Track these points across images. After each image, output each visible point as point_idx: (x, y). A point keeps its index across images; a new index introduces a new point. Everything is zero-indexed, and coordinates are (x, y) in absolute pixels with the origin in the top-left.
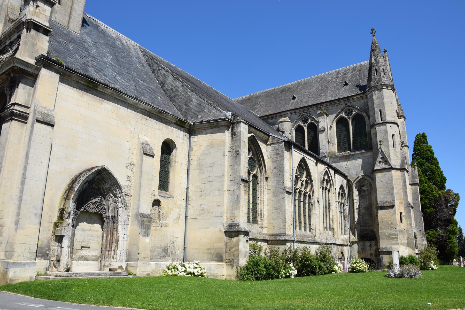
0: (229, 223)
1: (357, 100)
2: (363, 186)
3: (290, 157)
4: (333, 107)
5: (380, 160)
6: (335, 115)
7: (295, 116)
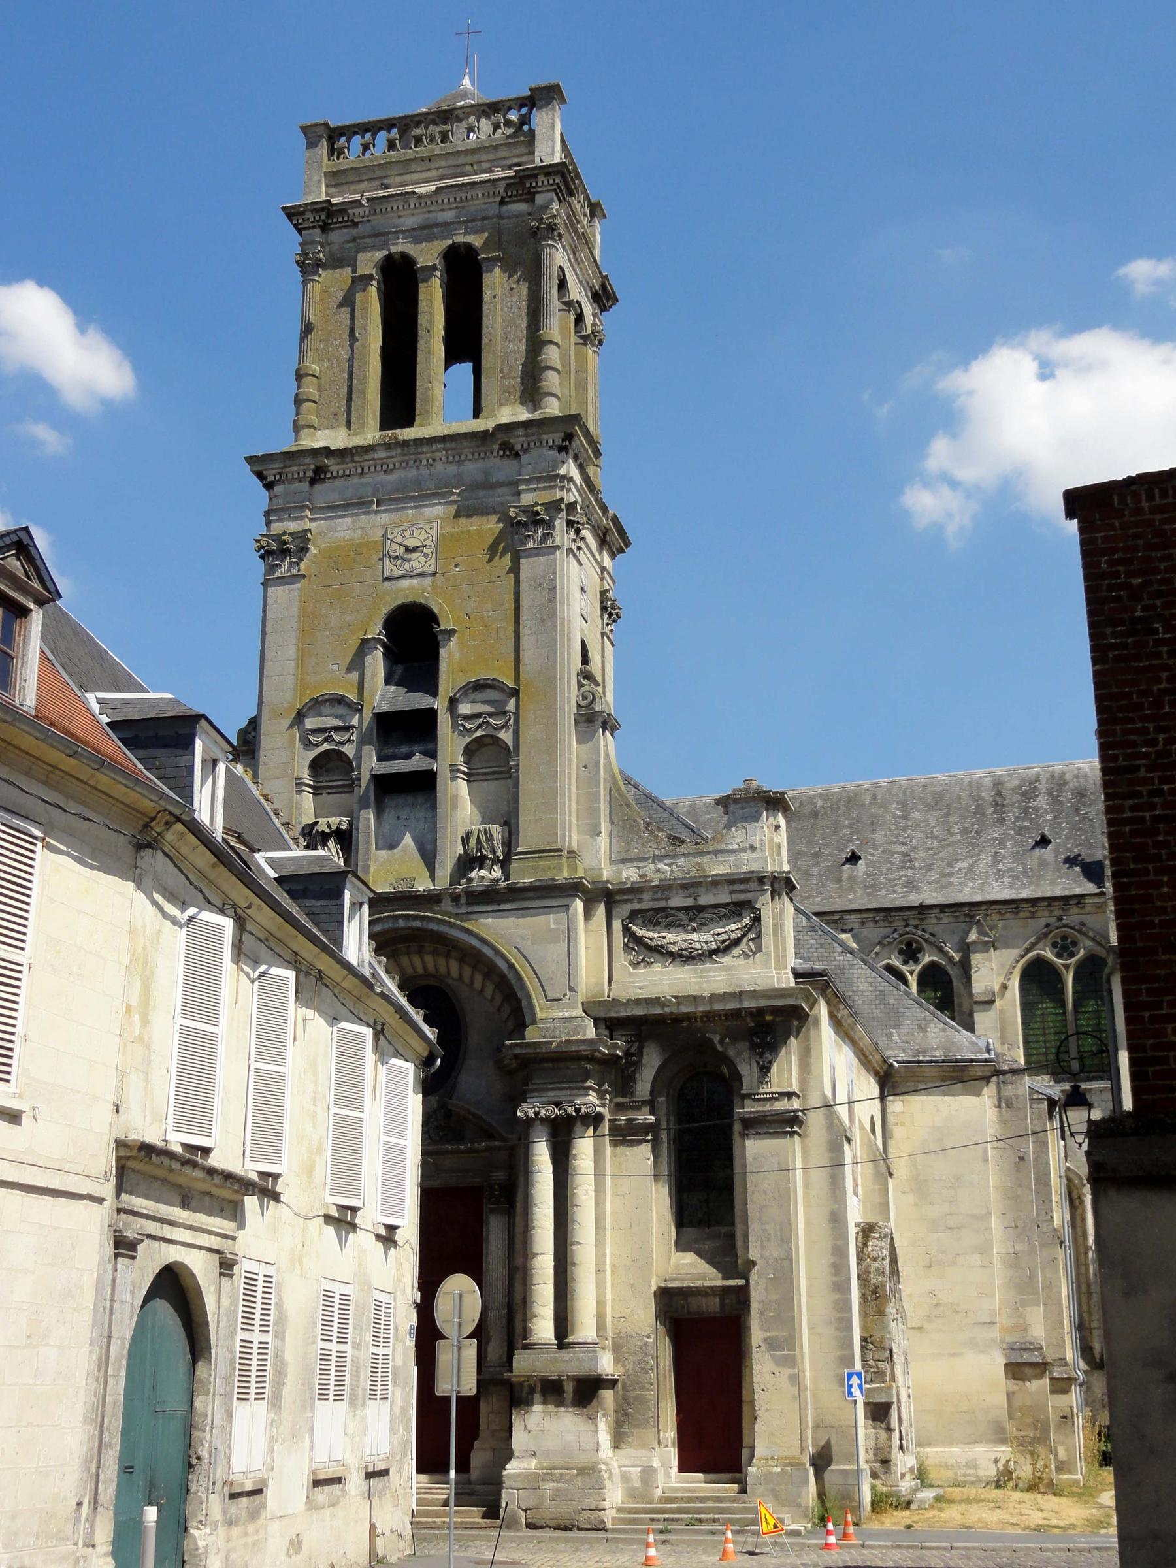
0: (1009, 1339)
1: (1093, 910)
4: (1013, 922)
7: (873, 933)
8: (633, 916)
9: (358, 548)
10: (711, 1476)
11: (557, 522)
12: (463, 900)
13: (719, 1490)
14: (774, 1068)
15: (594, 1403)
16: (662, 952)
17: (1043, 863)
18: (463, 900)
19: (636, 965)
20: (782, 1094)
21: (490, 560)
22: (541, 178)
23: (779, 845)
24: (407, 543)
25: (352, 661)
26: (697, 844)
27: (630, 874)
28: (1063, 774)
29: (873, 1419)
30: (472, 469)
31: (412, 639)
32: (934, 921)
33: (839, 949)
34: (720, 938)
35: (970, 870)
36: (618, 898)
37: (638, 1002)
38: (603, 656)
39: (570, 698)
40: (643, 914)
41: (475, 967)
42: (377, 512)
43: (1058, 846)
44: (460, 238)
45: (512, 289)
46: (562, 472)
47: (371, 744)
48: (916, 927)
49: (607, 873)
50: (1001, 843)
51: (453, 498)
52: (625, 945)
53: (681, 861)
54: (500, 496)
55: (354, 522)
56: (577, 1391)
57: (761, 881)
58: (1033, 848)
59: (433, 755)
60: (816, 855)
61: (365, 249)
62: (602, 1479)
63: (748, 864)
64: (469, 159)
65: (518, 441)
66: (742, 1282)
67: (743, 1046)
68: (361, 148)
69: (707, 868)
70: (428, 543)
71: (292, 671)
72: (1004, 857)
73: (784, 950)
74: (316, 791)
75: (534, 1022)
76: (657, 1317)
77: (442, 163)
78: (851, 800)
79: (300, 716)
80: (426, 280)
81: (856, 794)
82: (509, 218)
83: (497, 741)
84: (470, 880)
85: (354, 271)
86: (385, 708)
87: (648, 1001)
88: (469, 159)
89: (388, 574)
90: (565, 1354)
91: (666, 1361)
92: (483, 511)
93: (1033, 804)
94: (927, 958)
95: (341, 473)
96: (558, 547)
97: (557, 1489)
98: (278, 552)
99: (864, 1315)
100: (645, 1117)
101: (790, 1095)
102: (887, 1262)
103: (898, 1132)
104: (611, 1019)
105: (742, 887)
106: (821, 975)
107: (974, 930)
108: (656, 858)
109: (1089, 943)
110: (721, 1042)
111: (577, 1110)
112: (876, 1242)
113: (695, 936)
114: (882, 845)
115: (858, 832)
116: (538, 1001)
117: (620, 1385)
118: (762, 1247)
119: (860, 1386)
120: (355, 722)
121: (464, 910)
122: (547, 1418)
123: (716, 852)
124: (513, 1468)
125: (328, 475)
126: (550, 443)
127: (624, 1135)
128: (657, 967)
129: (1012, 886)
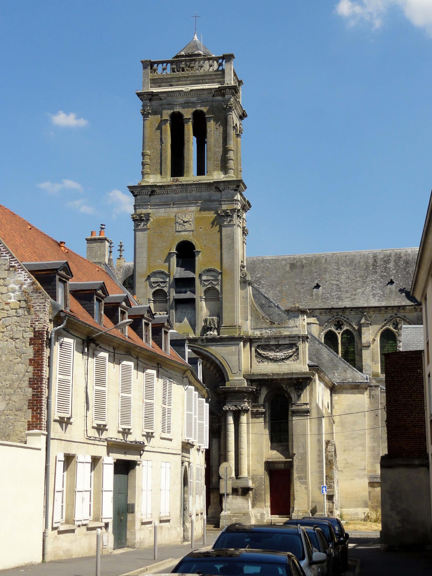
0: (370, 474)
4: (378, 315)
6: (379, 326)
7: (324, 317)
8: (258, 347)
9: (167, 220)
10: (280, 516)
11: (234, 215)
12: (205, 341)
13: (282, 520)
14: (302, 396)
15: (248, 495)
16: (267, 358)
17: (391, 292)
18: (205, 341)
19: (259, 362)
20: (304, 404)
21: (212, 227)
22: (227, 90)
23: (304, 326)
24: (184, 219)
25: (166, 259)
26: (279, 324)
27: (257, 333)
28: (400, 253)
29: (328, 500)
30: (205, 194)
31: (186, 253)
32: (348, 314)
33: (318, 343)
34: (286, 355)
35: (363, 293)
36: (254, 341)
37: (260, 375)
38: (243, 250)
39: (238, 275)
40: (262, 346)
41: (207, 361)
42: (173, 207)
43: (397, 284)
44: (199, 108)
45: (217, 128)
46: (235, 198)
47: (173, 288)
48: (341, 316)
49: (250, 333)
50: (375, 282)
51: (199, 204)
52: (256, 356)
53: (274, 330)
54: (215, 205)
55: (165, 210)
56: (242, 491)
57: (299, 337)
58: (387, 285)
59: (194, 292)
60: (303, 284)
61: (165, 109)
62: (250, 516)
63: (295, 332)
64: (201, 78)
65: (221, 187)
66: (291, 460)
67: (292, 389)
68: (162, 70)
69: (282, 332)
70: (191, 220)
71: (146, 262)
72: (376, 288)
73: (306, 359)
74: (154, 302)
75: (228, 381)
76: (265, 470)
77: (192, 79)
78: (316, 261)
79: (149, 277)
80: (187, 123)
81: (319, 258)
82: (216, 102)
83: (215, 289)
84: (207, 335)
85: (161, 117)
86: (177, 276)
87: (263, 375)
88: (201, 78)
89: (177, 230)
90: (238, 481)
91: (268, 483)
92: (209, 209)
93: (388, 266)
94: (345, 328)
95: (160, 193)
96: (235, 225)
97: (237, 520)
98: (139, 220)
99: (326, 469)
100: (262, 410)
101: (307, 404)
102: (333, 453)
103: (336, 406)
104: (252, 379)
105: (293, 339)
106: (317, 366)
107: (363, 318)
108: (266, 328)
110: (286, 387)
111: (242, 408)
112: (330, 447)
113: (278, 354)
114: (329, 281)
115: (320, 275)
116: (229, 374)
117: (254, 490)
118: (297, 449)
119: (326, 490)
120: (168, 280)
121: (205, 344)
122: (233, 499)
123: (285, 327)
124: (223, 513)
125: (156, 193)
126: (232, 188)
127: (255, 415)
128: (266, 363)
129: (379, 300)
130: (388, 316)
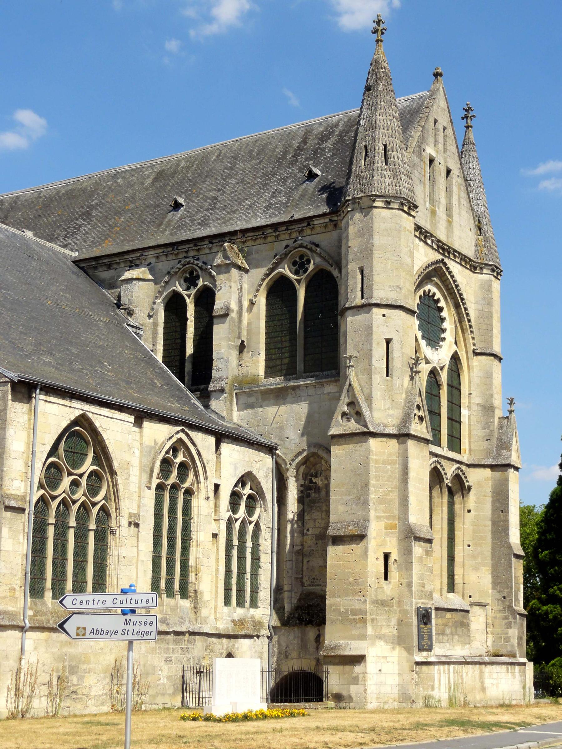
1: (322, 230)
2: (316, 476)
3: (29, 420)
4: (262, 247)
5: (345, 409)
6: (263, 271)
7: (164, 265)
32: (207, 251)
109: (318, 260)
130: (280, 247)
